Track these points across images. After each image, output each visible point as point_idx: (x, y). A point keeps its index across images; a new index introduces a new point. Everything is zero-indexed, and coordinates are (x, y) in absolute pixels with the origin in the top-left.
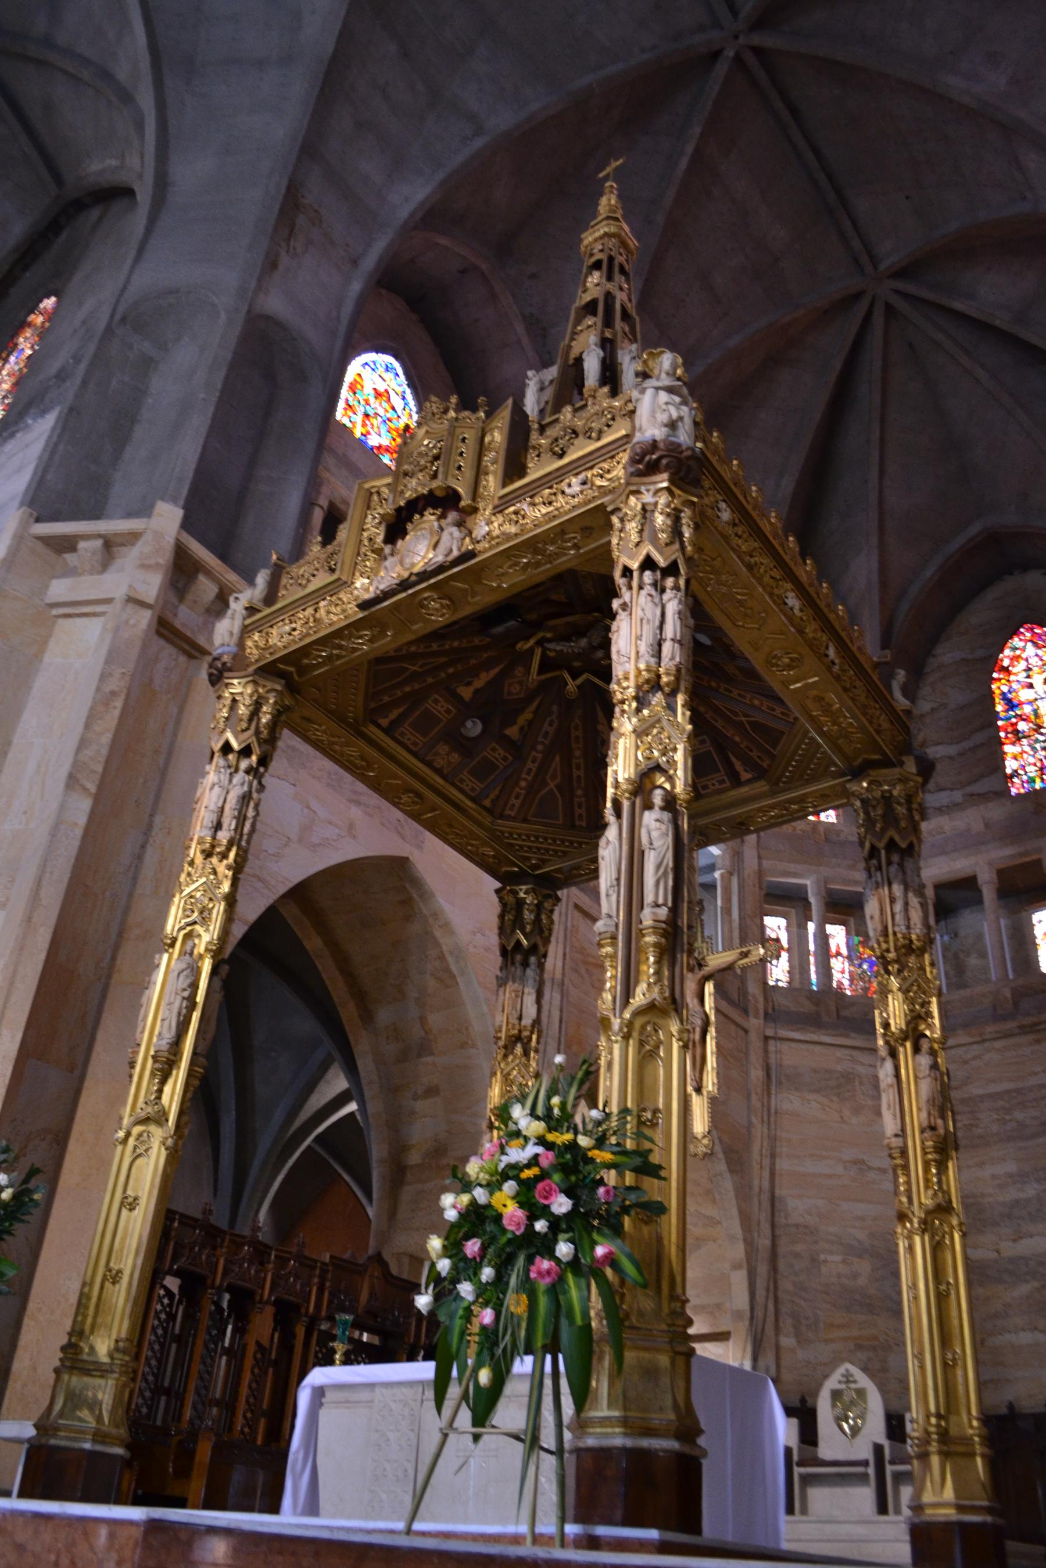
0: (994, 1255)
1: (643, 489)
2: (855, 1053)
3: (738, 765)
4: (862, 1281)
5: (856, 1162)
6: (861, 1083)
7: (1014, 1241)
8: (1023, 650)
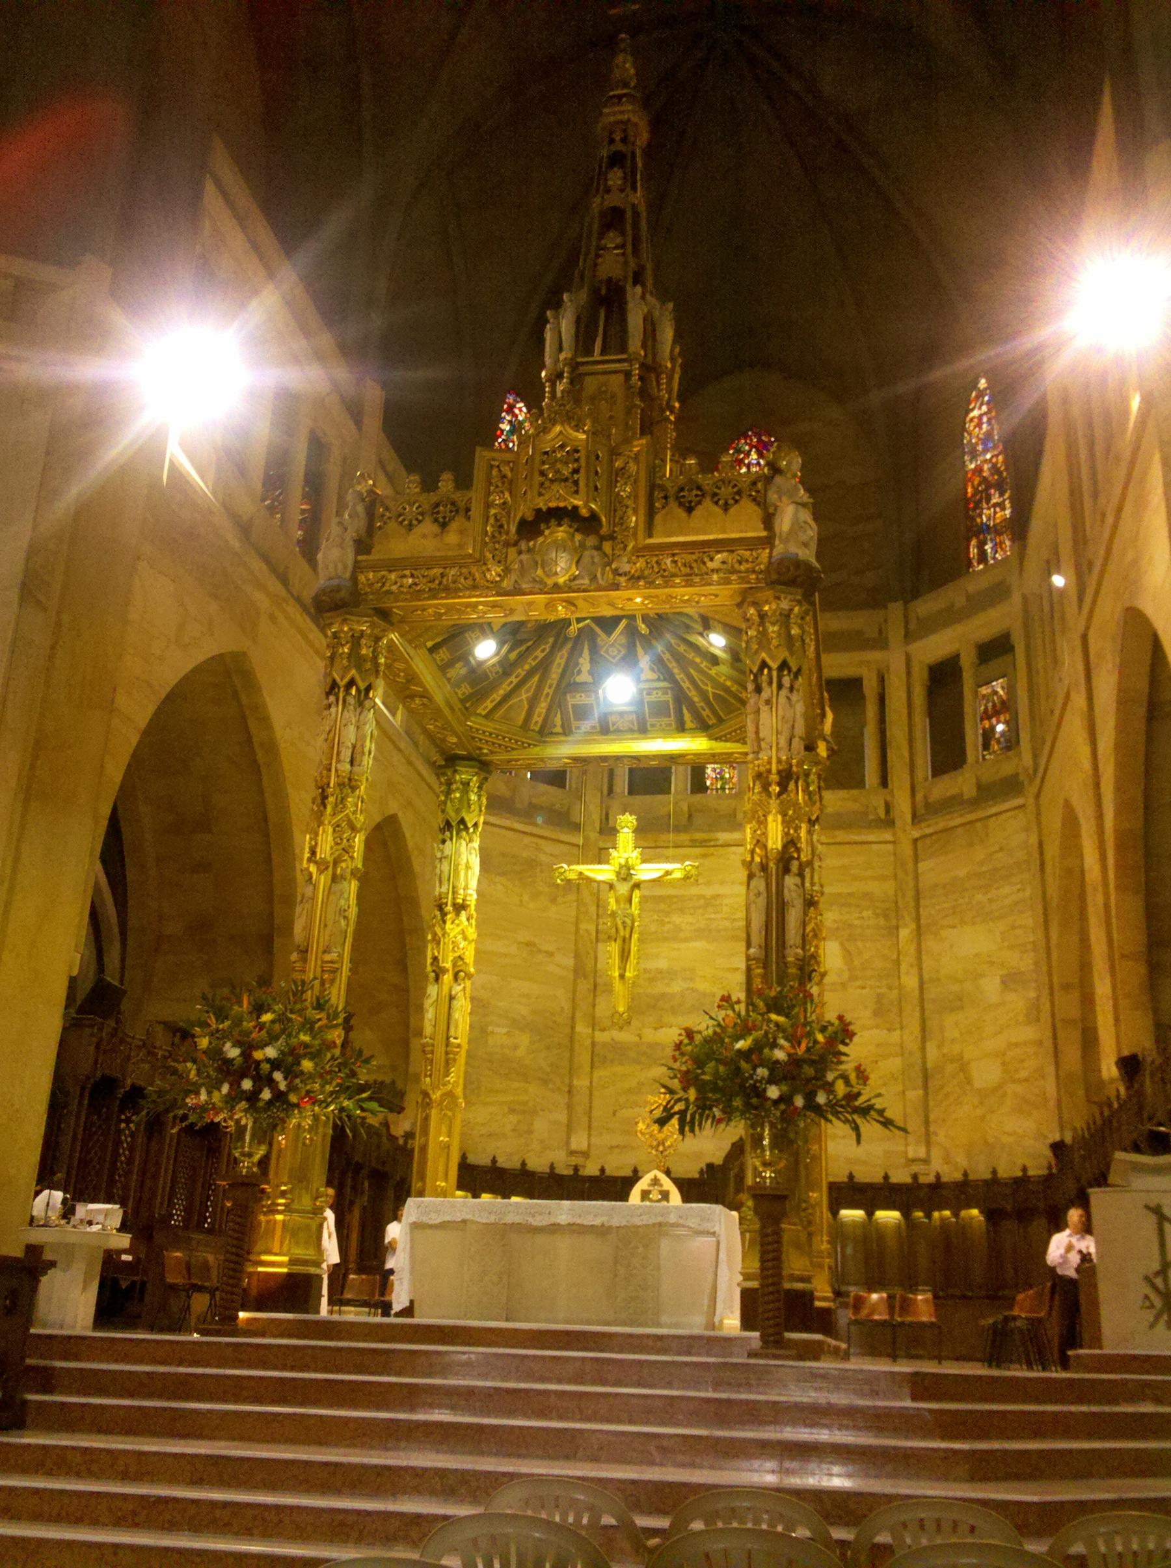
0: (637, 1039)
1: (782, 596)
2: (541, 842)
3: (687, 716)
4: (521, 1052)
5: (528, 944)
6: (542, 871)
7: (656, 1029)
8: (748, 454)
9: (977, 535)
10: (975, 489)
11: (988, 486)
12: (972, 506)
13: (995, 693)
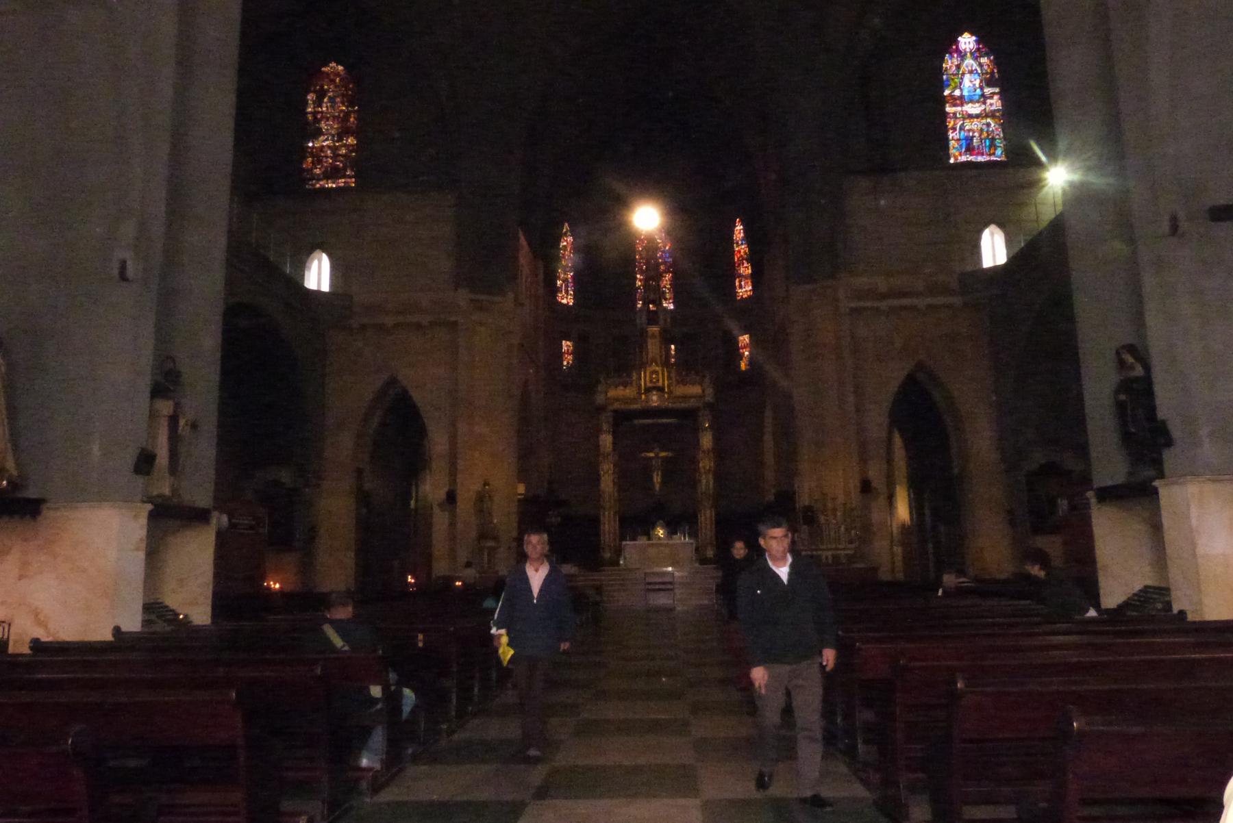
9: (738, 277)
10: (738, 259)
11: (743, 259)
12: (737, 265)
13: (745, 340)
